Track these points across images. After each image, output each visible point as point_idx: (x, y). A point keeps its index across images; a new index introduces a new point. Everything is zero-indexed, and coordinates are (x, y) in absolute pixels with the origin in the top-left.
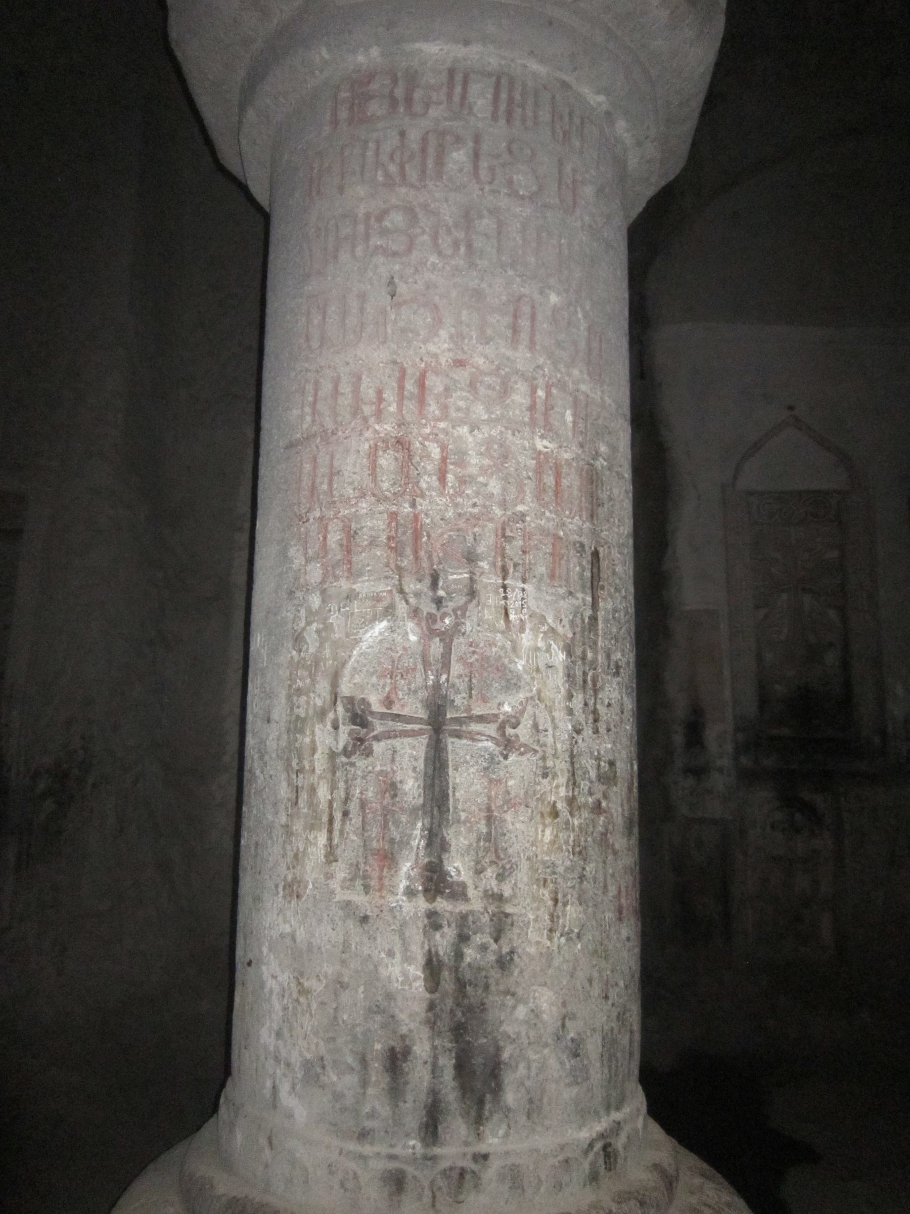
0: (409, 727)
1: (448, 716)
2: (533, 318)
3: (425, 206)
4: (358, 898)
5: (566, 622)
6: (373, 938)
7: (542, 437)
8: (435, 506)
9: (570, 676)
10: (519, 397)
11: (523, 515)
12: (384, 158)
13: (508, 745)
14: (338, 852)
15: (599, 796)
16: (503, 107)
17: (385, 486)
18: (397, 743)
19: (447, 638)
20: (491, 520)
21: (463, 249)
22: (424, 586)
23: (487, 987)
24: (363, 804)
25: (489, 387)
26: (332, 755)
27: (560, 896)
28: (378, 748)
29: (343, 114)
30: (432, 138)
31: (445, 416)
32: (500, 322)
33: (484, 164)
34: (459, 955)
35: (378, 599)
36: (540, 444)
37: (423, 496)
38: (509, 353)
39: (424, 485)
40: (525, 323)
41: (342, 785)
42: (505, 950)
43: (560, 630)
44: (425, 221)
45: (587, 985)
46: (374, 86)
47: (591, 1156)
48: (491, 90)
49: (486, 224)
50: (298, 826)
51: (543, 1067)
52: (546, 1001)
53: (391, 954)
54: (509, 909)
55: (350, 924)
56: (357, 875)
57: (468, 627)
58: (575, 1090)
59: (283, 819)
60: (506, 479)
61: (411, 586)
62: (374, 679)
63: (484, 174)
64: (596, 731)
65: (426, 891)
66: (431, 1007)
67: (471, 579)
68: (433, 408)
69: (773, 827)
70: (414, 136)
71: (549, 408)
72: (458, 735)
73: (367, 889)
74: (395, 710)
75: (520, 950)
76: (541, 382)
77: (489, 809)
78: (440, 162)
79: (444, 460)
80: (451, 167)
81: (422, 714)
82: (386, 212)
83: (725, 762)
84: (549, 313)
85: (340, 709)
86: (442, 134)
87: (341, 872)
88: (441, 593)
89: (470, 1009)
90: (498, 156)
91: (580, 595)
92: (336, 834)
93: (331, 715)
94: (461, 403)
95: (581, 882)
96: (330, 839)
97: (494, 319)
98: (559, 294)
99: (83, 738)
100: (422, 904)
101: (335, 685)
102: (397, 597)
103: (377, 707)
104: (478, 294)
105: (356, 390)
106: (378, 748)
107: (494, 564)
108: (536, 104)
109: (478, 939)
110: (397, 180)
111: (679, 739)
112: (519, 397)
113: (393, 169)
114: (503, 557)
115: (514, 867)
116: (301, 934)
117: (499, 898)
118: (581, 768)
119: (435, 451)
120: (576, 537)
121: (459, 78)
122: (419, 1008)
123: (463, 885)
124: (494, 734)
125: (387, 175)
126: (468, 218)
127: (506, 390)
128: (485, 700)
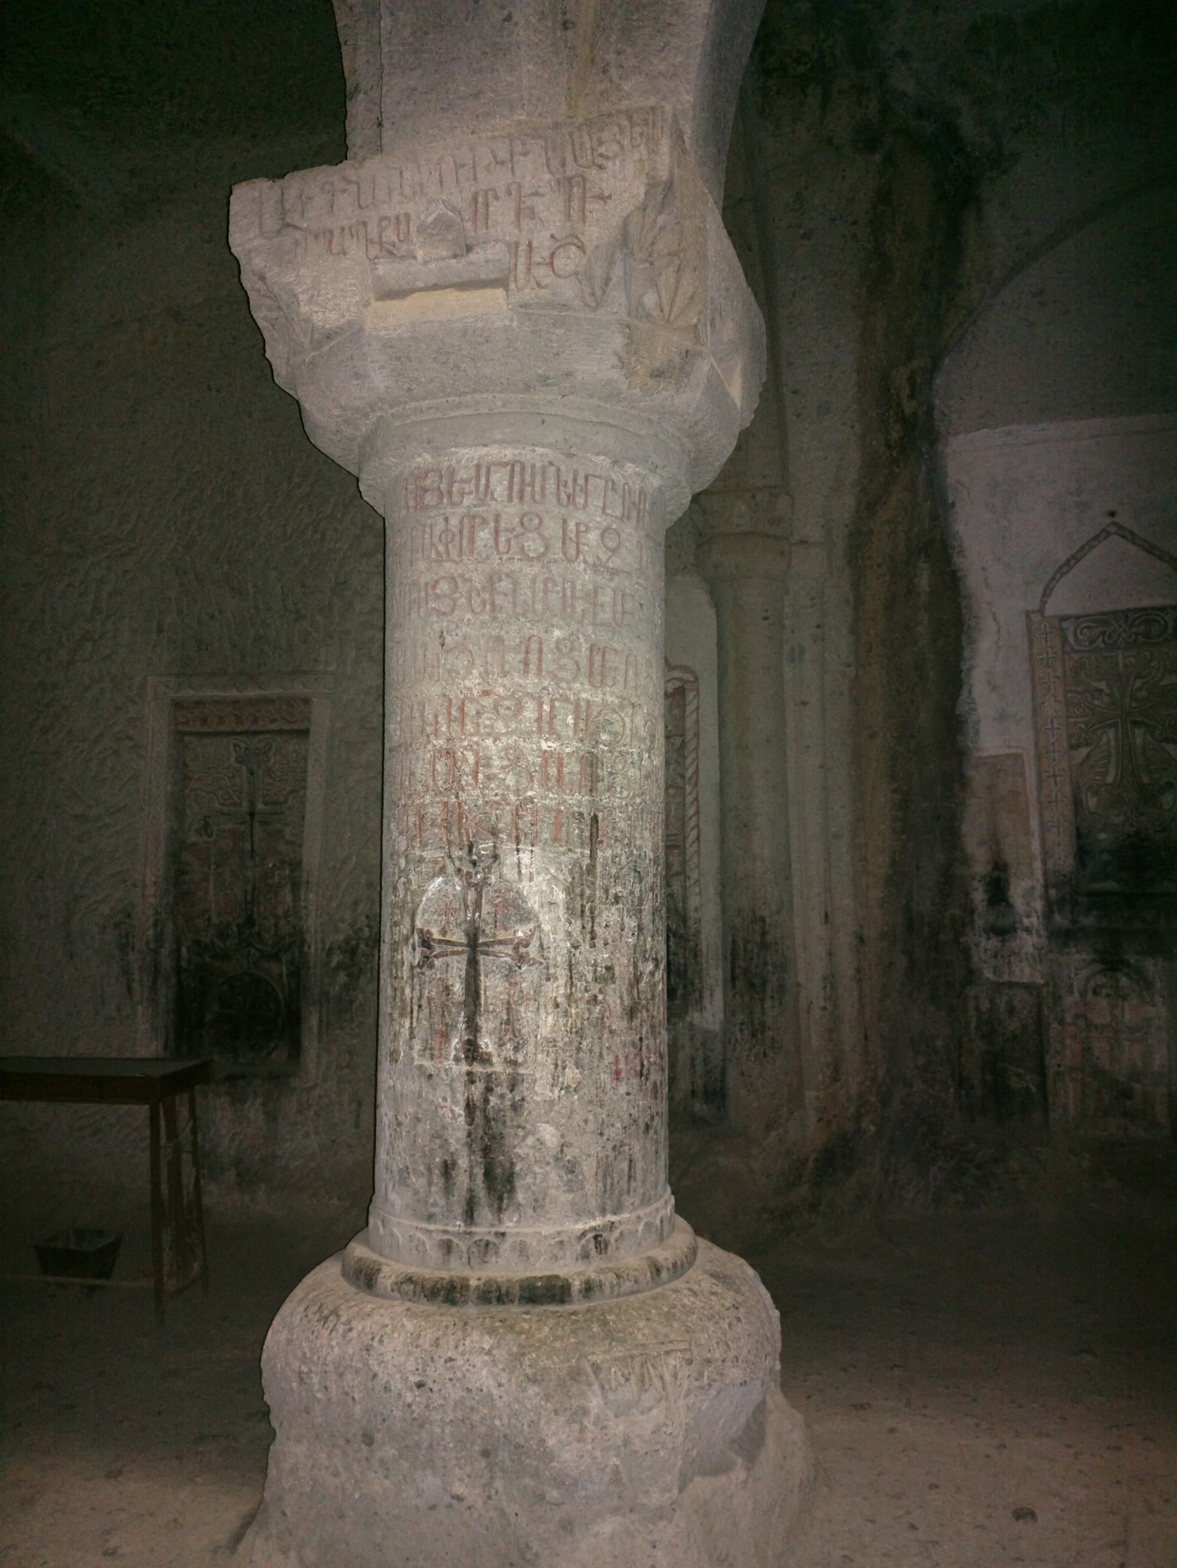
0: (456, 949)
1: (481, 940)
2: (540, 651)
3: (462, 576)
4: (427, 1063)
5: (565, 871)
6: (434, 1089)
7: (547, 740)
8: (471, 795)
9: (569, 909)
10: (530, 712)
11: (531, 800)
12: (436, 539)
13: (521, 959)
14: (415, 1032)
15: (596, 991)
16: (516, 488)
17: (440, 783)
18: (449, 959)
19: (479, 888)
20: (508, 804)
21: (488, 607)
22: (463, 853)
23: (504, 1123)
24: (429, 1000)
25: (508, 708)
26: (412, 968)
27: (559, 1063)
28: (437, 962)
29: (412, 503)
30: (466, 521)
31: (477, 733)
32: (514, 658)
33: (502, 539)
34: (486, 1101)
35: (436, 862)
36: (544, 746)
37: (463, 790)
38: (521, 681)
39: (463, 783)
40: (533, 657)
41: (417, 987)
42: (517, 1098)
43: (561, 877)
44: (463, 587)
45: (582, 1124)
46: (428, 482)
47: (583, 1241)
48: (507, 477)
49: (505, 585)
50: (396, 1016)
51: (546, 1176)
52: (549, 1134)
53: (445, 1099)
54: (521, 1071)
55: (423, 1079)
56: (427, 1049)
57: (493, 879)
58: (570, 1196)
59: (389, 1010)
60: (519, 775)
61: (457, 853)
62: (436, 917)
63: (502, 547)
64: (593, 946)
65: (467, 1057)
66: (469, 1135)
67: (494, 847)
68: (470, 727)
69: (1095, 993)
70: (454, 521)
71: (552, 717)
72: (487, 954)
73: (432, 1057)
74: (448, 938)
75: (528, 1099)
76: (546, 699)
77: (508, 1002)
78: (472, 540)
79: (477, 763)
80: (479, 543)
81: (464, 940)
82: (437, 582)
83: (1034, 921)
84: (553, 645)
85: (416, 936)
86: (474, 517)
87: (417, 1045)
88: (474, 857)
89: (493, 1137)
90: (514, 529)
91: (579, 850)
92: (415, 1020)
93: (411, 941)
94: (488, 722)
95: (578, 1053)
96: (411, 1023)
97: (510, 657)
98: (561, 628)
99: (367, 917)
100: (464, 1067)
101: (413, 921)
102: (448, 861)
103: (436, 935)
104: (499, 639)
105: (422, 716)
106: (437, 962)
107: (509, 835)
108: (544, 480)
109: (499, 1090)
110: (444, 556)
111: (979, 896)
112: (530, 712)
113: (441, 548)
114: (517, 829)
115: (525, 1042)
116: (398, 1086)
117: (514, 1063)
118: (578, 973)
119: (471, 759)
120: (576, 809)
121: (483, 470)
122: (461, 1135)
123: (489, 1054)
124: (510, 952)
125: (438, 552)
126: (492, 580)
127: (519, 708)
128: (506, 929)
